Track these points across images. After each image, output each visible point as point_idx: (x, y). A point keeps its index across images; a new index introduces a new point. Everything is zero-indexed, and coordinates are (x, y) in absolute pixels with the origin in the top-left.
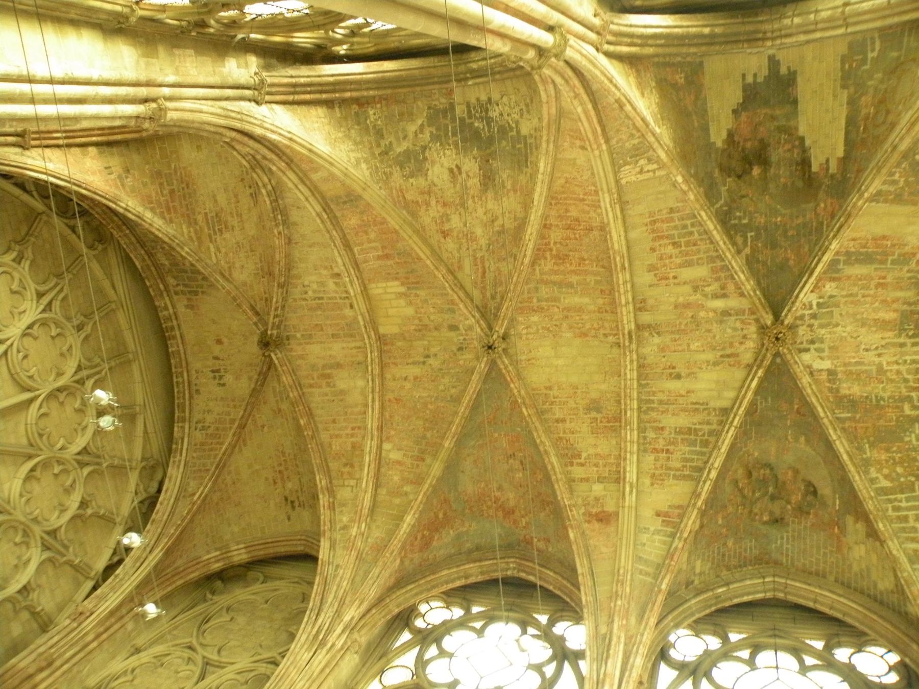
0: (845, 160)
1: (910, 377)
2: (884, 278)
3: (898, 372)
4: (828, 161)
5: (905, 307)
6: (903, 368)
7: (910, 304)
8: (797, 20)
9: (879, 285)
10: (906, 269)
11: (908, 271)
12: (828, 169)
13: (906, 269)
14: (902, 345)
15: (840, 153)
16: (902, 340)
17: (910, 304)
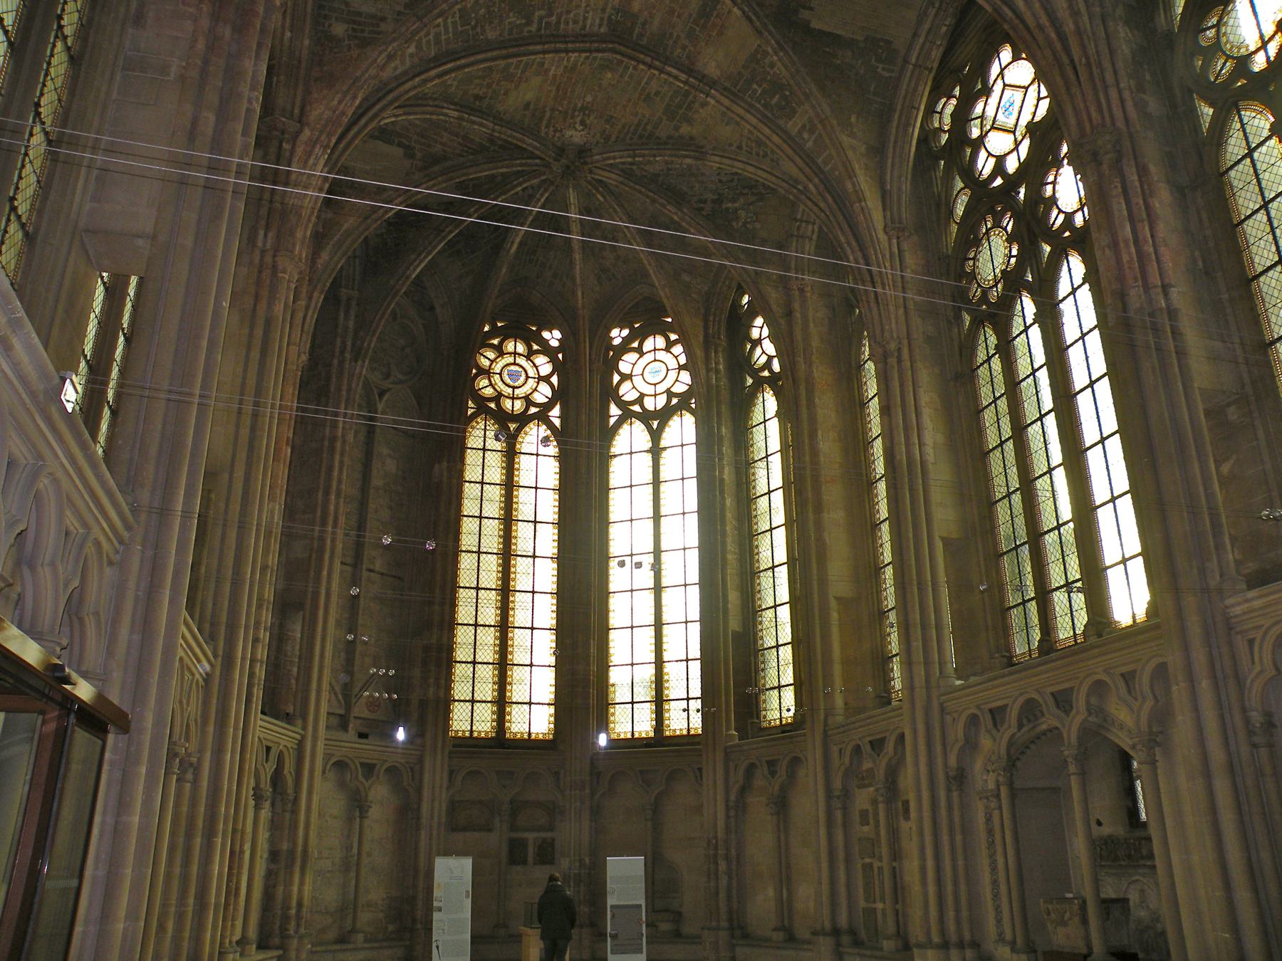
0: (806, 28)
1: (572, 15)
2: (679, 16)
3: (578, 6)
4: (811, 9)
5: (641, 20)
6: (581, 11)
7: (644, 24)
8: (944, 29)
9: (672, 12)
10: (683, 36)
11: (678, 36)
12: (804, 8)
13: (683, 36)
14: (604, 10)
15: (815, 24)
16: (608, 10)
17: (644, 24)
